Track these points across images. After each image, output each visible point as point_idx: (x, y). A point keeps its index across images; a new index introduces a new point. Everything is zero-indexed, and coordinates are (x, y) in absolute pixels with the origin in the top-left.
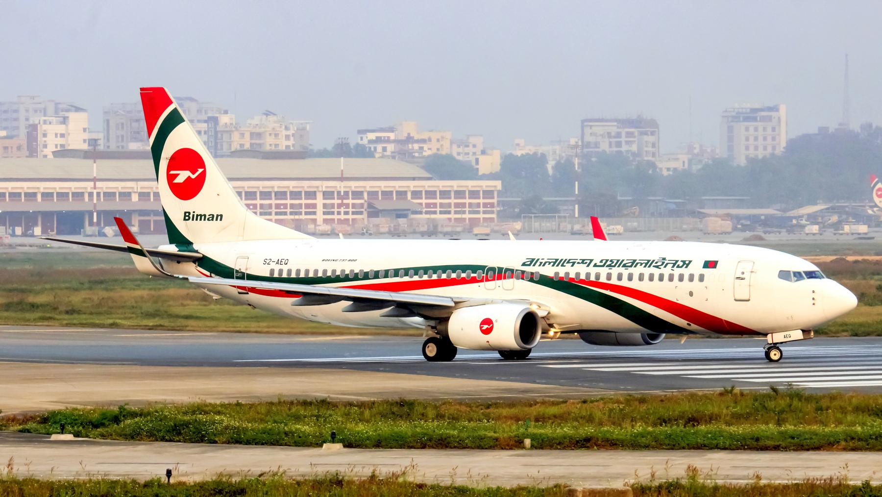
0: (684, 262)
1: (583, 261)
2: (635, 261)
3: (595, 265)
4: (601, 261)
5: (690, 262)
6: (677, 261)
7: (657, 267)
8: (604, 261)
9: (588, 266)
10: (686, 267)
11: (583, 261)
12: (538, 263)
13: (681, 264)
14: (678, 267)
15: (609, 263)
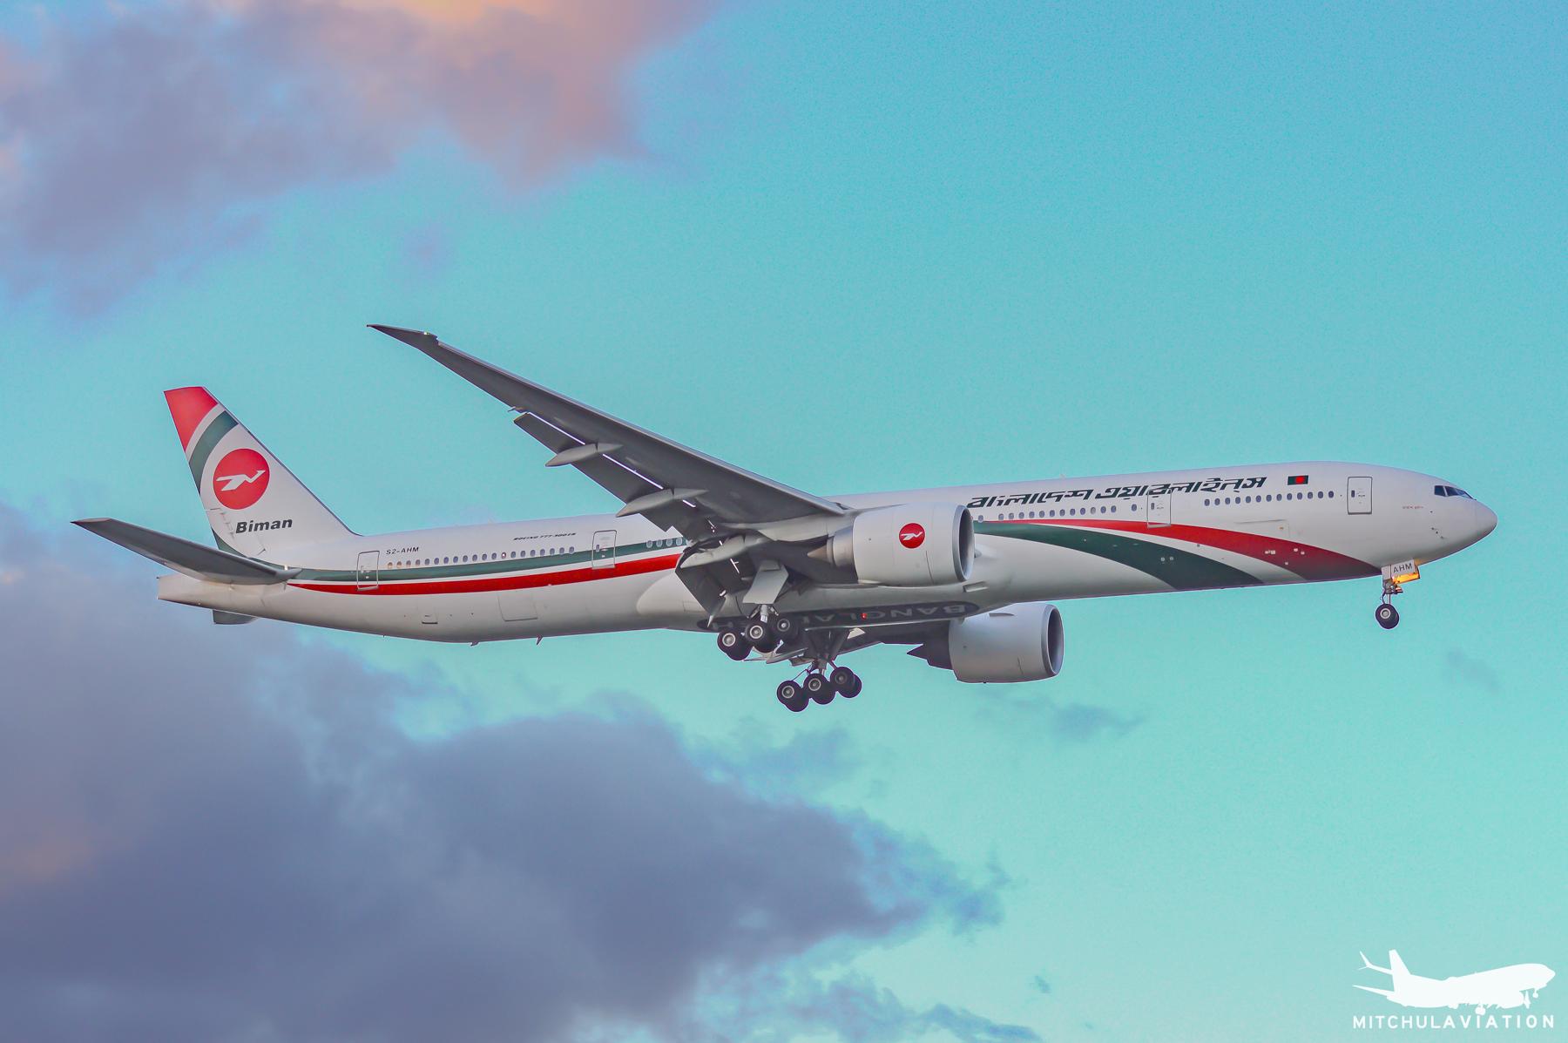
0: (1254, 481)
1: (1075, 494)
2: (1167, 486)
3: (1099, 496)
4: (1108, 491)
5: (1263, 479)
6: (1240, 481)
7: (1209, 490)
8: (1113, 491)
9: (1086, 498)
10: (1260, 485)
11: (1075, 494)
12: (996, 502)
13: (1249, 483)
14: (1245, 486)
15: (1121, 492)
